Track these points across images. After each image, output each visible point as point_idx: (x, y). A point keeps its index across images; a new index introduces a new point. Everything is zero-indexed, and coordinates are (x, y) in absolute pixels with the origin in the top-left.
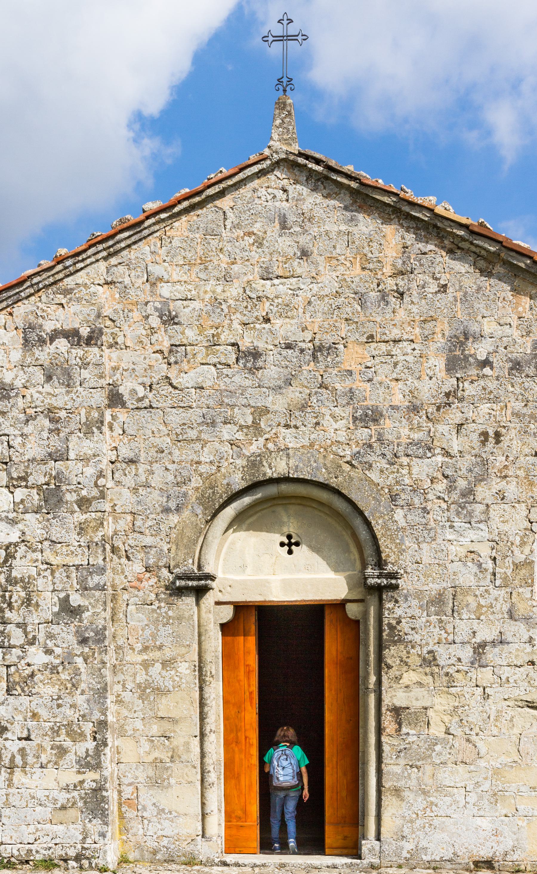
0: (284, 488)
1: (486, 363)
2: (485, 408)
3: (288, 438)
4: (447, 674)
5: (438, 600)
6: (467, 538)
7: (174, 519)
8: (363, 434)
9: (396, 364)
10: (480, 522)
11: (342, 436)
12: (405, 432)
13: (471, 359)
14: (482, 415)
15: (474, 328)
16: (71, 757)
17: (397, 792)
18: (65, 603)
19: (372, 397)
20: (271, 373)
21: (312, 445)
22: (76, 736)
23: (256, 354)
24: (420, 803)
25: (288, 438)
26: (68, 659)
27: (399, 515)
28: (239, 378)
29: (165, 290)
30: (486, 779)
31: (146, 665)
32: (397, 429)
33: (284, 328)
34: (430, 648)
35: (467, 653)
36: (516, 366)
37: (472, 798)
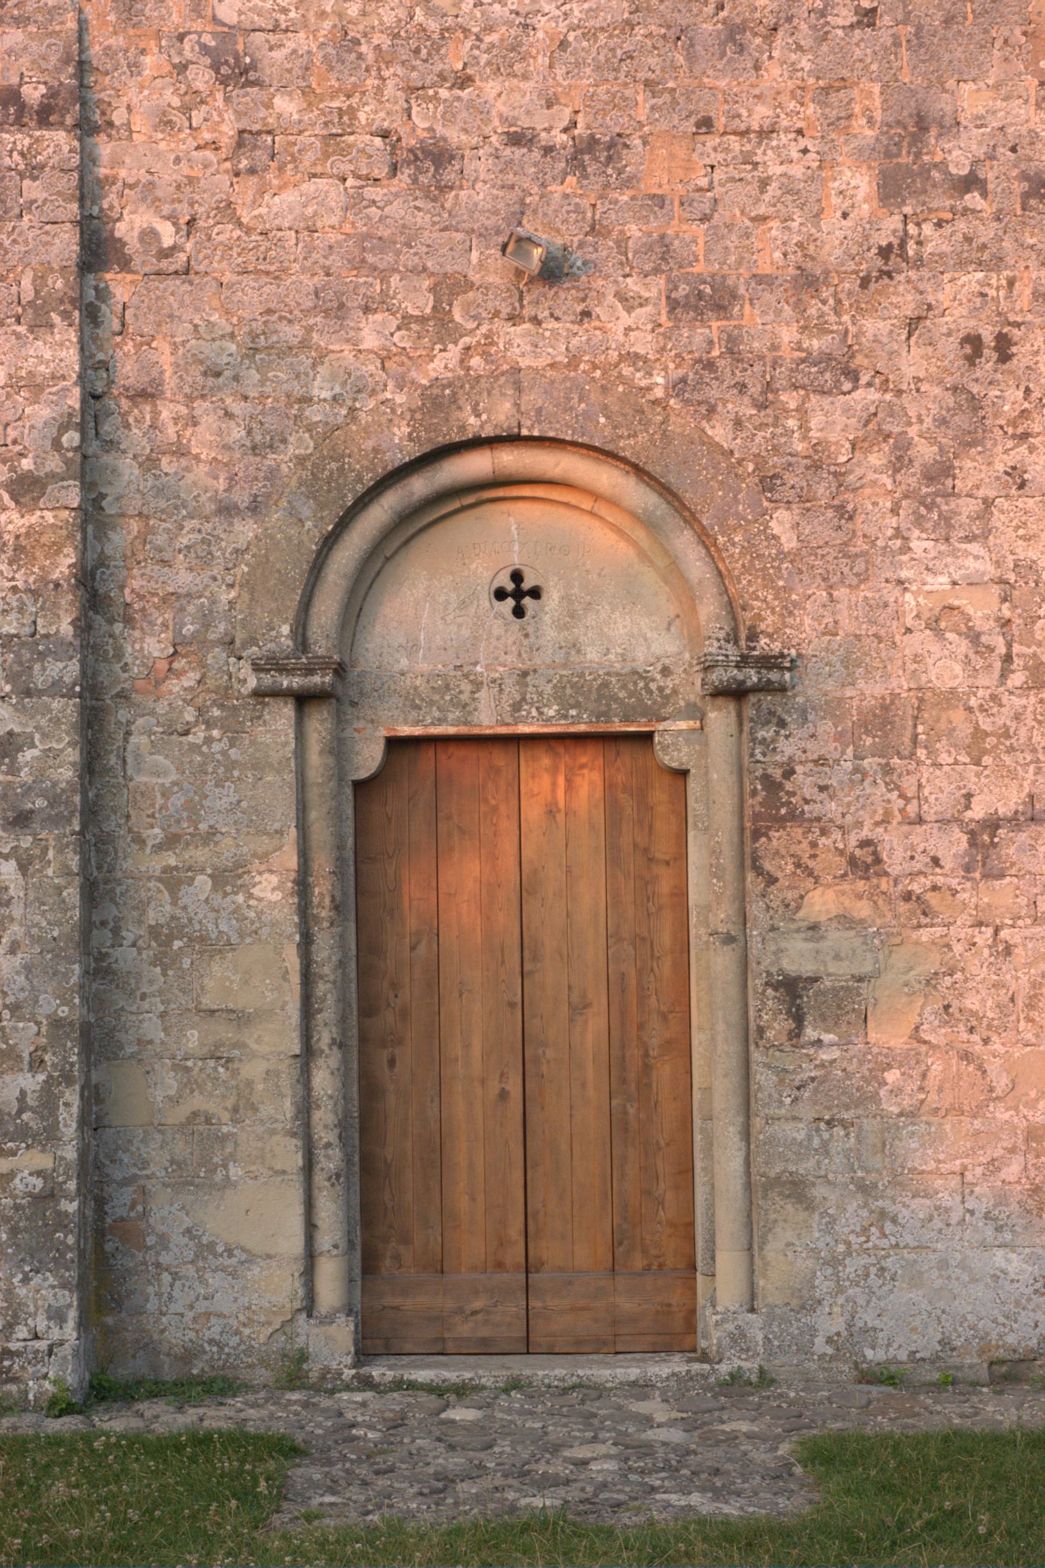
1: (971, 182)
4: (908, 896)
5: (882, 718)
9: (764, 183)
10: (968, 539)
11: (644, 343)
12: (788, 335)
13: (936, 175)
15: (943, 104)
21: (574, 362)
27: (781, 523)
30: (1012, 1150)
34: (865, 833)
35: (953, 845)
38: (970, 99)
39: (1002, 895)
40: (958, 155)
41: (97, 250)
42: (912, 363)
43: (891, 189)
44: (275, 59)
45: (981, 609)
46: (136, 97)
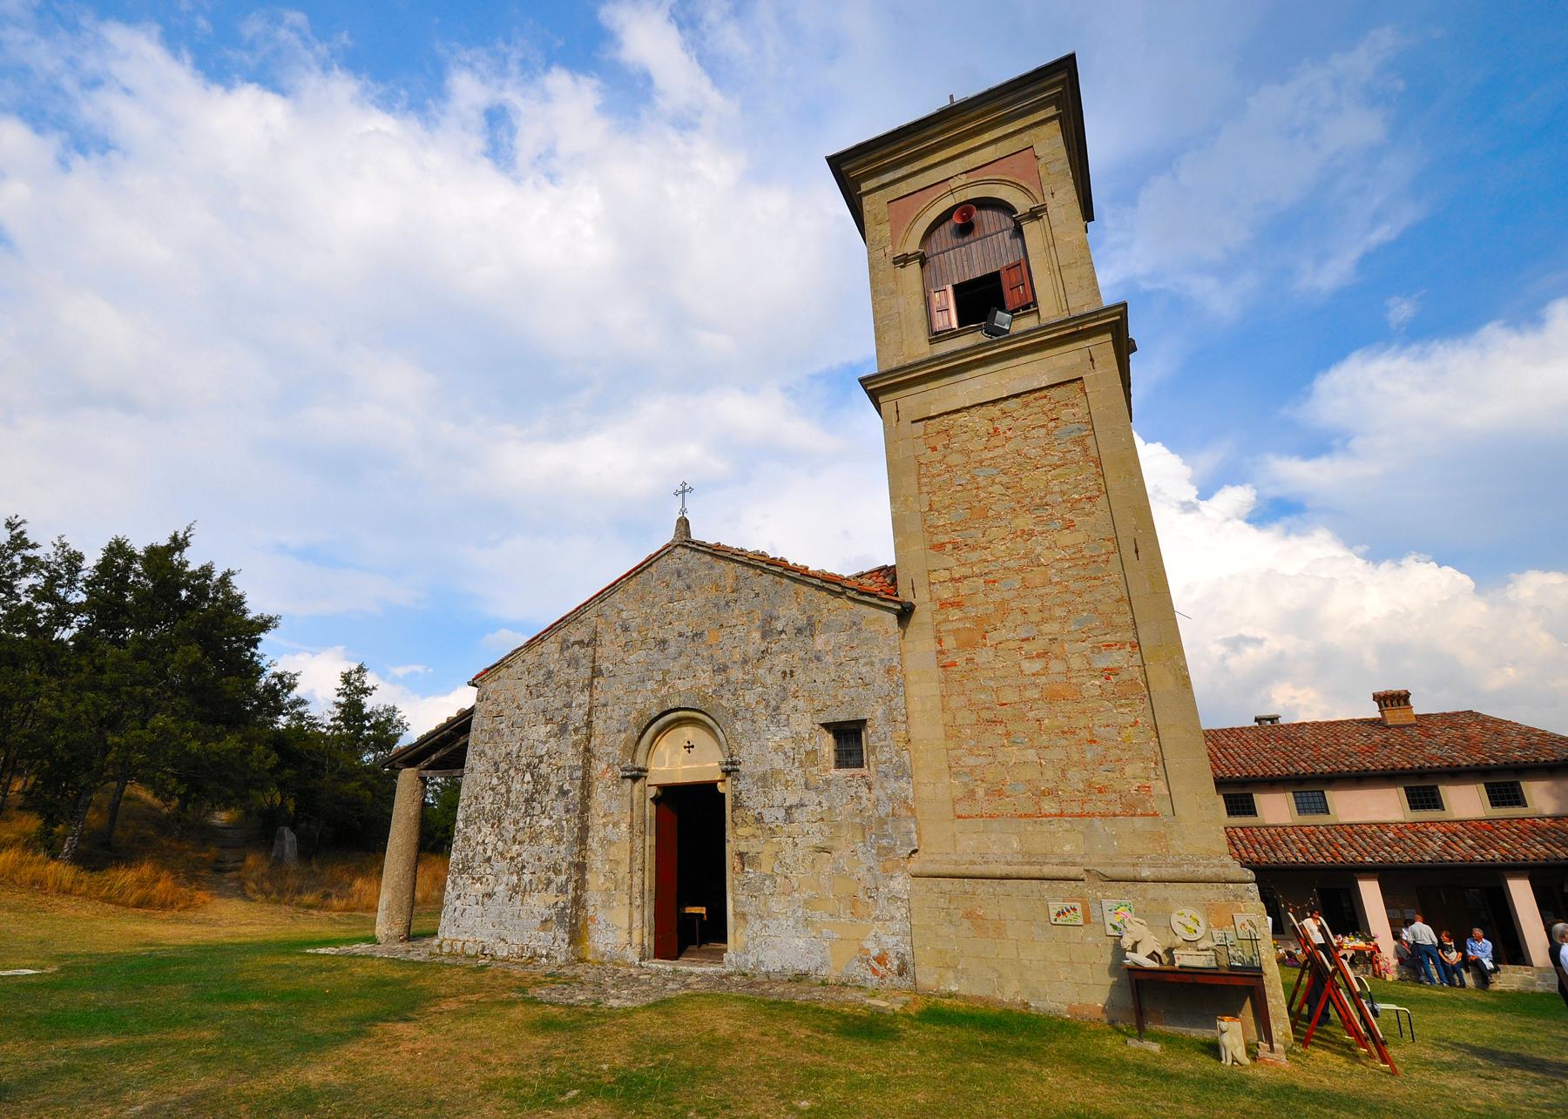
0: (680, 714)
2: (783, 657)
3: (680, 685)
6: (777, 736)
7: (623, 736)
8: (719, 678)
12: (741, 676)
14: (781, 662)
15: (775, 613)
16: (553, 886)
17: (743, 916)
18: (561, 788)
19: (720, 657)
20: (672, 650)
22: (557, 872)
23: (664, 642)
24: (758, 925)
25: (680, 685)
26: (561, 819)
27: (738, 725)
28: (656, 655)
29: (624, 615)
31: (605, 825)
32: (736, 674)
33: (679, 626)
35: (781, 814)
36: (799, 631)
37: (791, 922)
38: (781, 611)
40: (779, 626)
41: (596, 672)
42: (769, 680)
43: (764, 637)
45: (788, 746)
46: (606, 638)
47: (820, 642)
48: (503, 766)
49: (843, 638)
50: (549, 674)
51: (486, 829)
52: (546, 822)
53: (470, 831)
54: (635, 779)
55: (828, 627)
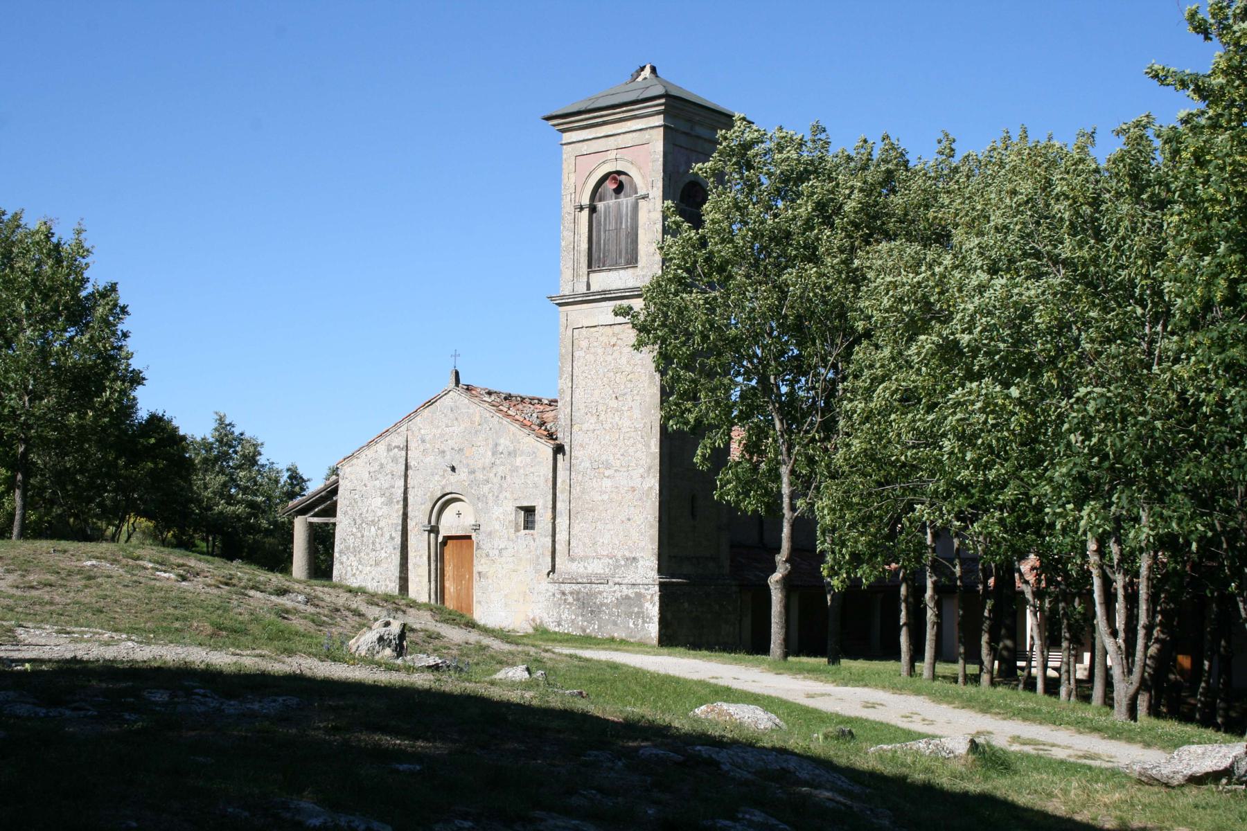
5: (490, 534)
14: (501, 470)
28: (439, 459)
32: (480, 476)
35: (497, 552)
38: (502, 441)
39: (503, 559)
40: (500, 449)
42: (495, 480)
43: (493, 454)
44: (427, 438)
45: (502, 517)
46: (412, 445)
47: (518, 461)
48: (359, 521)
49: (528, 460)
50: (382, 466)
51: (352, 558)
52: (383, 555)
53: (344, 559)
54: (430, 532)
55: (522, 453)
